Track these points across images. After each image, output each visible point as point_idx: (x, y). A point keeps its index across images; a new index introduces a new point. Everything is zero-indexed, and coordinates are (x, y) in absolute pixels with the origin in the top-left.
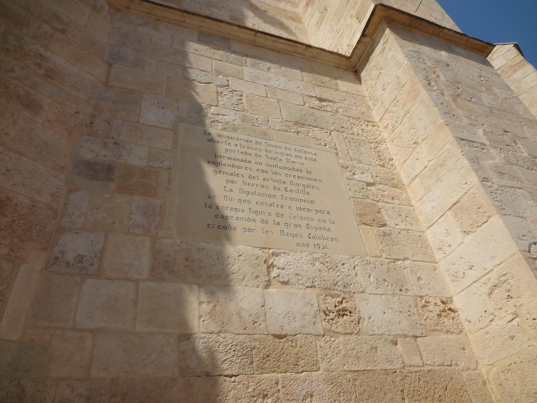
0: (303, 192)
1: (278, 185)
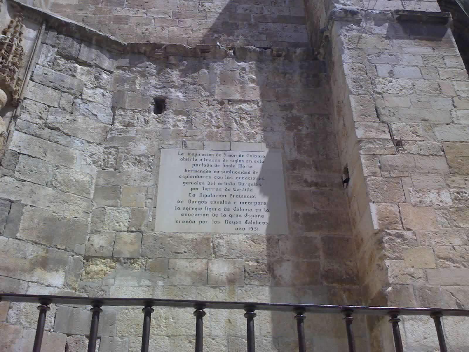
0: (248, 189)
1: (228, 187)
